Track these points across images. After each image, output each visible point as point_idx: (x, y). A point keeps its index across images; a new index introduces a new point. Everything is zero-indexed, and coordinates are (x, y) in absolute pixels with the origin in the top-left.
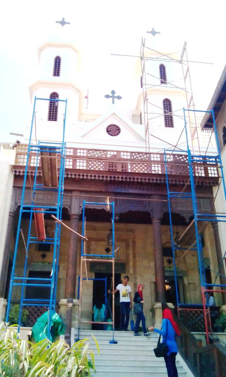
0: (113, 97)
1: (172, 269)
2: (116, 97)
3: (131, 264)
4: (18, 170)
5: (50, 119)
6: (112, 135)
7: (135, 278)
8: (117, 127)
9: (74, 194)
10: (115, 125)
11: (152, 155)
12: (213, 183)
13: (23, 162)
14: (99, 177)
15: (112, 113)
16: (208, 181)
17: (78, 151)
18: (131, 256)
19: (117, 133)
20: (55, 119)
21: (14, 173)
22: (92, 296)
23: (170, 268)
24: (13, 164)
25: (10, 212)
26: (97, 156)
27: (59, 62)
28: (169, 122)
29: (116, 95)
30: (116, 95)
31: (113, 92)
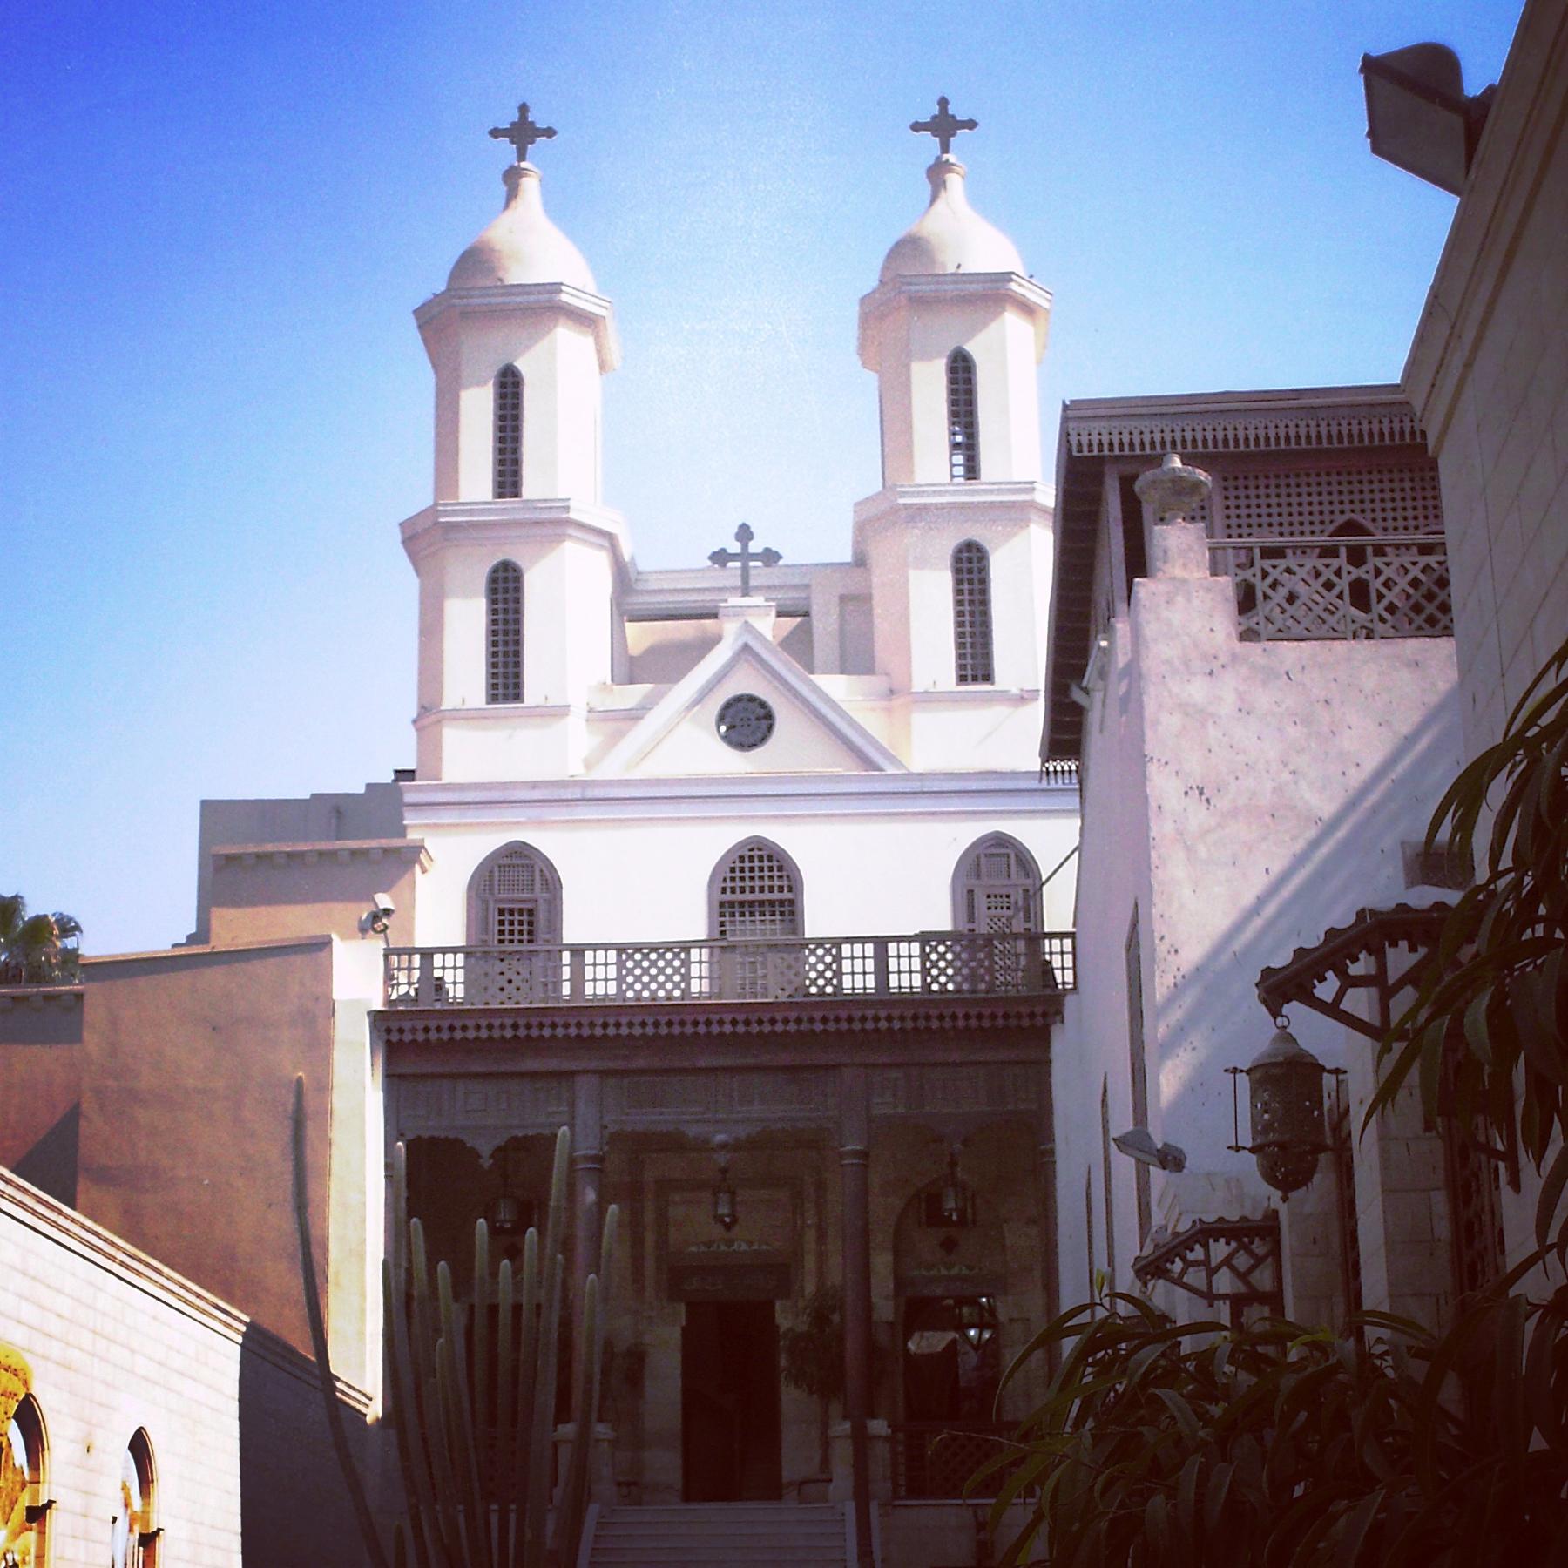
0: (745, 556)
1: (955, 1271)
2: (755, 557)
8: (763, 705)
9: (585, 1086)
10: (752, 699)
12: (1044, 1015)
14: (656, 1024)
18: (810, 1236)
19: (759, 736)
21: (384, 1036)
24: (378, 1005)
27: (517, 396)
28: (975, 661)
29: (755, 547)
30: (755, 547)
31: (744, 533)
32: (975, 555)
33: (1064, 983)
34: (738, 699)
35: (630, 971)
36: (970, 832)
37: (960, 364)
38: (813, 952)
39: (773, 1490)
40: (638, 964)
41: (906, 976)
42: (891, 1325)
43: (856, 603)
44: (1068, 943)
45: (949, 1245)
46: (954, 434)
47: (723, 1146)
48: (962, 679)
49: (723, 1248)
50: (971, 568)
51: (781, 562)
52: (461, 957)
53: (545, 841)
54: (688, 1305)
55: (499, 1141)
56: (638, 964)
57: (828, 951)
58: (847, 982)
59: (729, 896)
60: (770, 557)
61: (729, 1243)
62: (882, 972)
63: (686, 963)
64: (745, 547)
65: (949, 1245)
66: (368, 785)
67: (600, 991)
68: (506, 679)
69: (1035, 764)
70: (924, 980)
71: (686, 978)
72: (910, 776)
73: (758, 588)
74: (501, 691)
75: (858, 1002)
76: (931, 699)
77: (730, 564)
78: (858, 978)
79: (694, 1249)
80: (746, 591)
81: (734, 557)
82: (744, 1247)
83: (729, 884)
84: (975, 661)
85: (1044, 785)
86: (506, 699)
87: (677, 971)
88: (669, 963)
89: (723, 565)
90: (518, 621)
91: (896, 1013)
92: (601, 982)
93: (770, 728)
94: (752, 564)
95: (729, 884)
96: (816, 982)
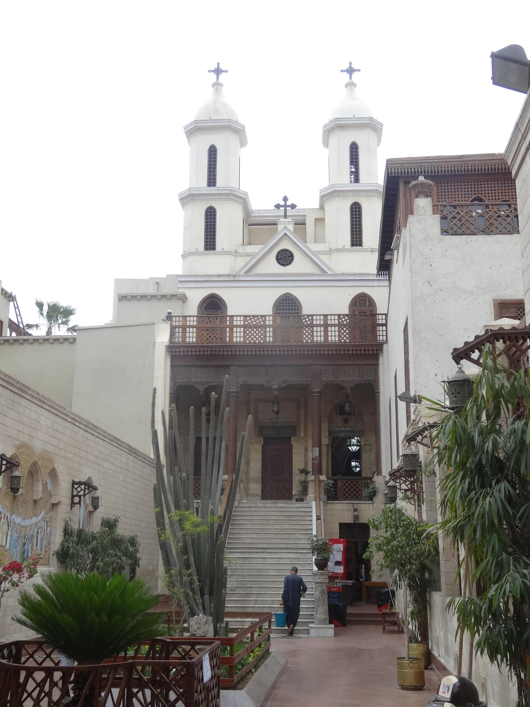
0: (285, 206)
1: (348, 429)
2: (289, 206)
3: (302, 426)
4: (174, 350)
5: (206, 249)
6: (283, 265)
7: (306, 441)
8: (290, 252)
10: (287, 250)
11: (315, 317)
12: (377, 350)
13: (178, 339)
15: (283, 233)
16: (371, 348)
17: (235, 318)
20: (214, 249)
22: (261, 462)
23: (346, 427)
25: (170, 394)
26: (254, 323)
27: (215, 154)
28: (357, 239)
29: (288, 203)
30: (288, 203)
31: (285, 199)
32: (357, 206)
33: (383, 340)
34: (283, 250)
35: (248, 334)
36: (355, 292)
37: (354, 146)
38: (305, 330)
39: (290, 497)
40: (250, 332)
41: (334, 336)
42: (327, 445)
43: (320, 221)
44: (384, 328)
45: (346, 421)
46: (352, 168)
47: (276, 389)
48: (352, 245)
49: (275, 420)
50: (356, 211)
51: (297, 208)
52: (195, 329)
53: (223, 294)
54: (264, 438)
55: (206, 386)
56: (250, 332)
57: (309, 329)
58: (315, 339)
59: (278, 311)
60: (293, 206)
61: (277, 419)
62: (326, 336)
63: (265, 332)
64: (285, 203)
65: (346, 421)
66: (167, 275)
67: (238, 340)
68: (210, 243)
69: (375, 272)
70: (339, 338)
71: (265, 337)
72: (336, 275)
73: (290, 216)
74: (209, 247)
75: (320, 345)
76: (343, 250)
77: (281, 208)
78: (318, 337)
79: (266, 420)
80: (285, 216)
81: (282, 206)
82: (282, 420)
83: (278, 308)
84: (357, 239)
85: (378, 278)
86: (210, 249)
87: (262, 334)
88: (260, 332)
89: (279, 209)
90: (215, 225)
91: (330, 349)
92: (238, 336)
93: (292, 259)
94: (287, 208)
95: (278, 308)
96: (306, 339)
